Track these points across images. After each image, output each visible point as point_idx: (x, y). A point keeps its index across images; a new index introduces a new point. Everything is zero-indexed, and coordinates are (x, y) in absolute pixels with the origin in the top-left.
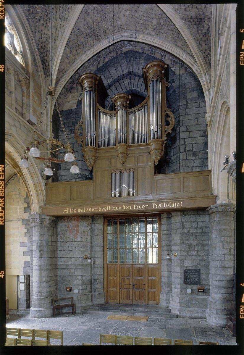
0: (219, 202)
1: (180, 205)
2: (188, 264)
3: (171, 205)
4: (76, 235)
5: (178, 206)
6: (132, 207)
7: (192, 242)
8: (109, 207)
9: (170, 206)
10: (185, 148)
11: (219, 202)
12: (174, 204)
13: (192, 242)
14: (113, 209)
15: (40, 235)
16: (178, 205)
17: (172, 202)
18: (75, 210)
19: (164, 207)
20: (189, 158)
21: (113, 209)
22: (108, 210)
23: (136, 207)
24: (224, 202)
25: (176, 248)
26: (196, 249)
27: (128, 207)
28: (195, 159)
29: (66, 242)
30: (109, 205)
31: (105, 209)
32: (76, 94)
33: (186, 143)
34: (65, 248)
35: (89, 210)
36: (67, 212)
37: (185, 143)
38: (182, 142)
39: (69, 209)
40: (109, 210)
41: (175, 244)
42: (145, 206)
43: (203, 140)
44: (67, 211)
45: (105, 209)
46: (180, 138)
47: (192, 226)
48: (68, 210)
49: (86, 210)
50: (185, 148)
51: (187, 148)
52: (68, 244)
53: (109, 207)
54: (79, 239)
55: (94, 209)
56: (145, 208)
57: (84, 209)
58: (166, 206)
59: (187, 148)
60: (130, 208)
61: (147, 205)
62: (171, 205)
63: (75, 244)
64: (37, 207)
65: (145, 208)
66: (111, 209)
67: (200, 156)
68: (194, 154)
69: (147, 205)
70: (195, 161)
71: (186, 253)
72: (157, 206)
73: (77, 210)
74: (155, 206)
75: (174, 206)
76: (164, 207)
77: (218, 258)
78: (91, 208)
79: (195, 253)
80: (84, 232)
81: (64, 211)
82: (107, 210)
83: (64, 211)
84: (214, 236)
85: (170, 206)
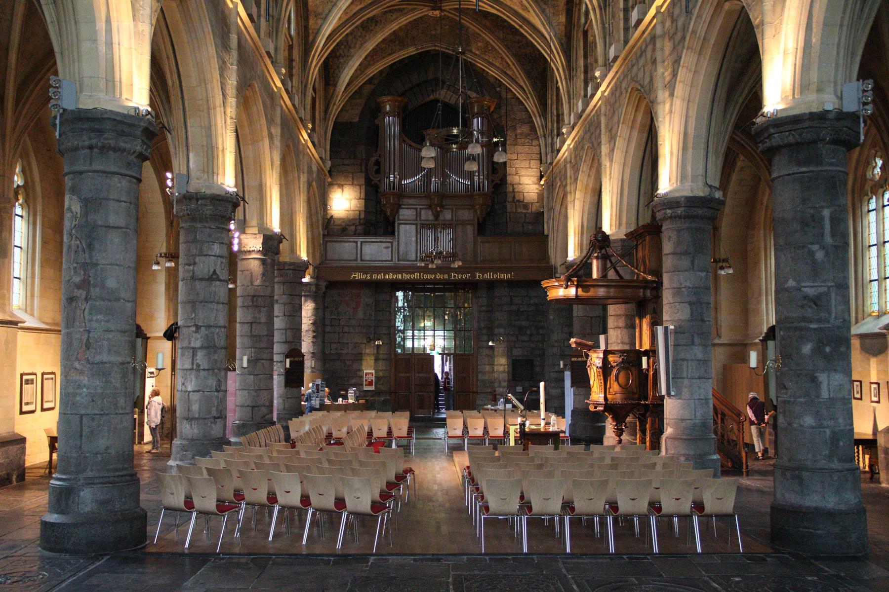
2: (516, 352)
4: (356, 309)
6: (450, 276)
7: (523, 323)
25: (502, 331)
26: (528, 332)
34: (337, 329)
41: (499, 326)
54: (360, 314)
60: (446, 276)
63: (353, 322)
71: (514, 339)
73: (371, 276)
77: (556, 344)
79: (526, 339)
80: (368, 305)
84: (551, 317)
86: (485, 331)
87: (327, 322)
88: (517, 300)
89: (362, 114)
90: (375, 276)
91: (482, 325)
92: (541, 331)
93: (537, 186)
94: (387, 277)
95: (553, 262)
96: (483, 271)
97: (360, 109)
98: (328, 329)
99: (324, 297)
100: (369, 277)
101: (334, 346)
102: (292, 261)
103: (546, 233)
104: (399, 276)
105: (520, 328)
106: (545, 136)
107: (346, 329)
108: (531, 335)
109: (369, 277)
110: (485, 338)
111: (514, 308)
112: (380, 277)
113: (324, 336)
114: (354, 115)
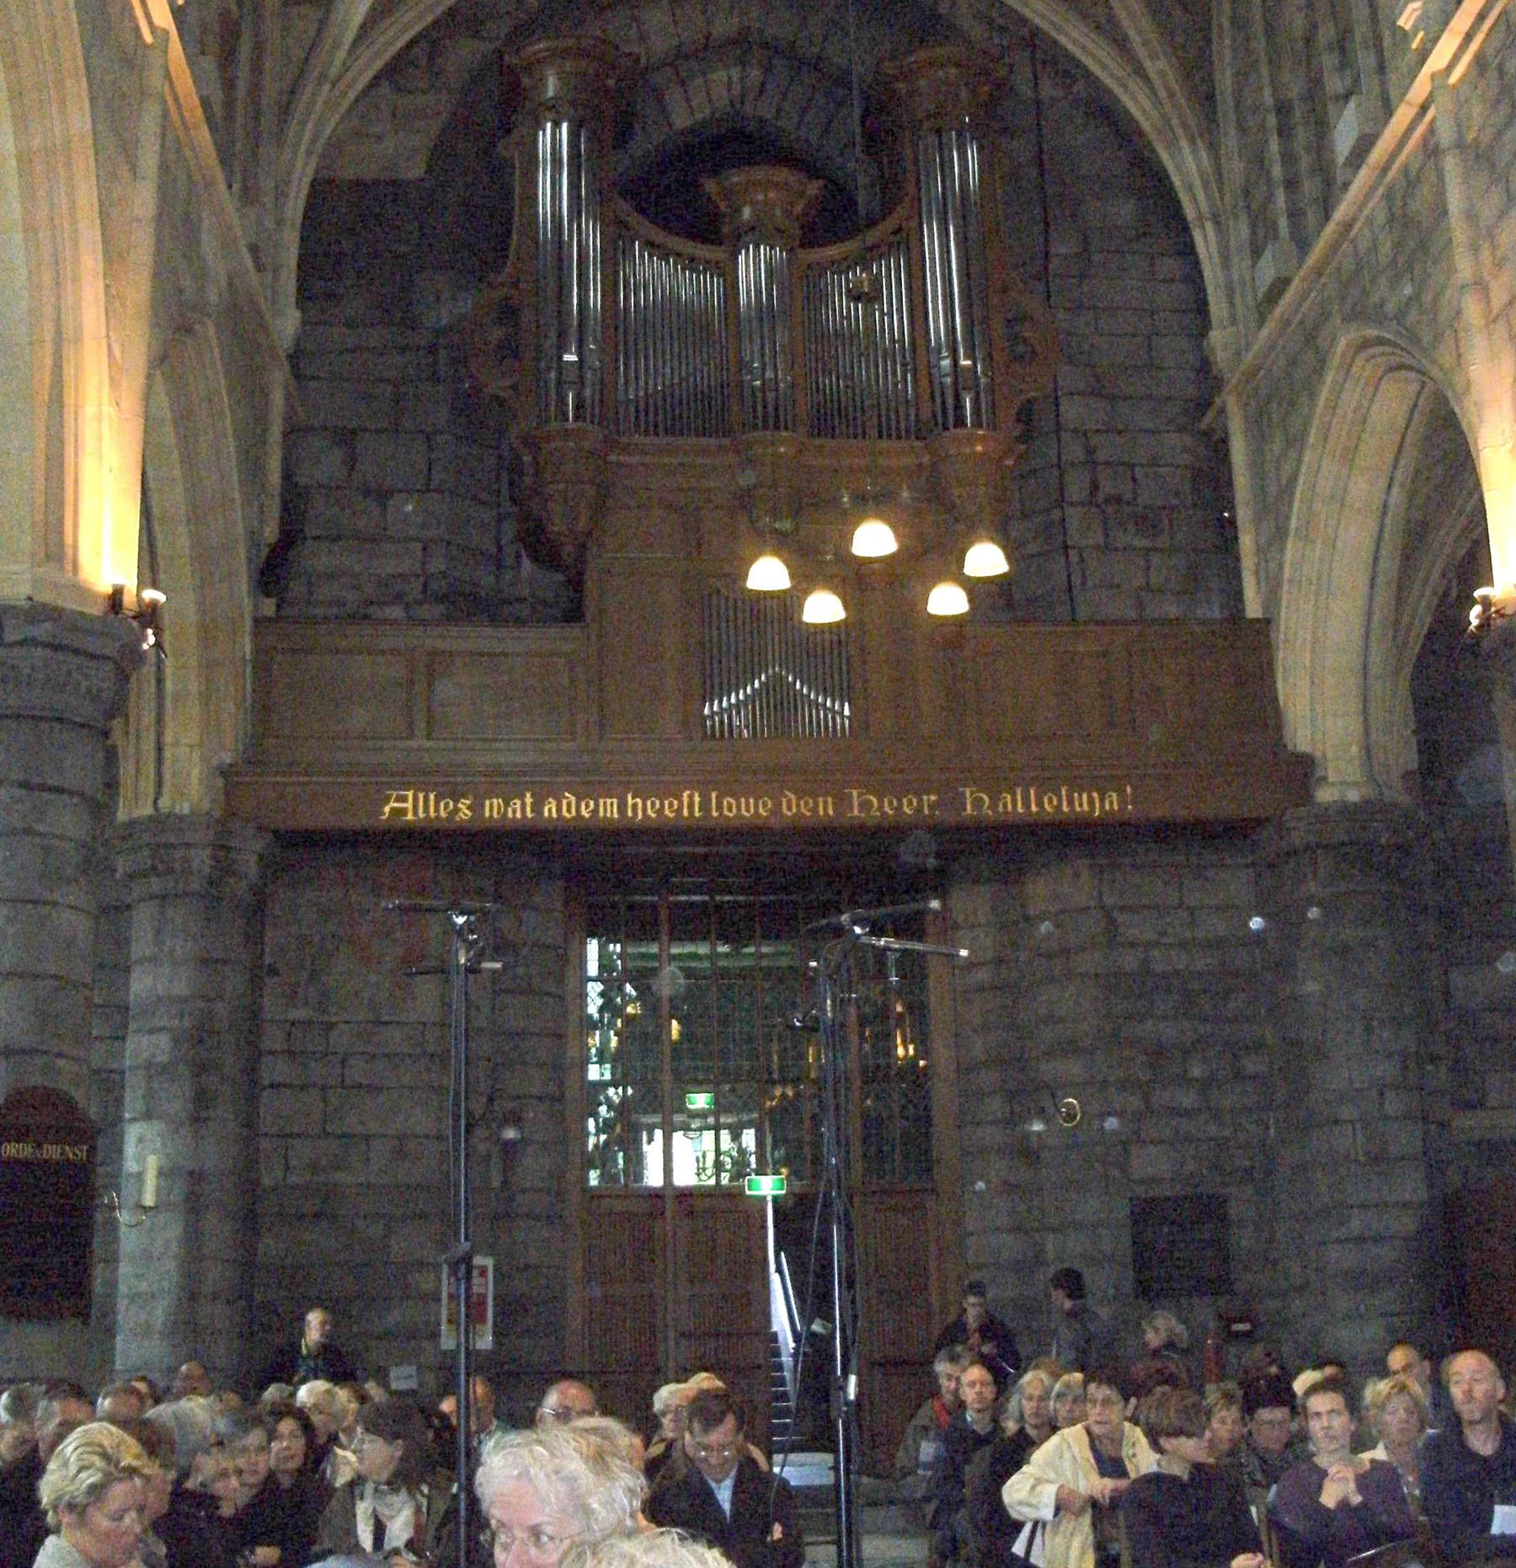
0: (1325, 795)
1: (1123, 802)
3: (1071, 803)
5: (1107, 807)
6: (842, 800)
8: (697, 799)
9: (1065, 808)
10: (1095, 487)
11: (1325, 795)
12: (1085, 796)
13: (1169, 1031)
14: (719, 807)
15: (205, 961)
16: (1111, 803)
17: (1076, 784)
18: (464, 805)
19: (1034, 808)
20: (1122, 539)
21: (719, 807)
22: (686, 813)
23: (865, 806)
24: (1353, 796)
27: (816, 804)
28: (1155, 549)
29: (331, 1026)
30: (691, 786)
31: (671, 805)
32: (421, 99)
33: (1101, 456)
35: (559, 809)
36: (410, 817)
37: (1090, 451)
38: (1074, 451)
39: (421, 796)
40: (697, 814)
42: (920, 801)
43: (1185, 450)
44: (409, 805)
45: (671, 805)
46: (1059, 428)
47: (1164, 934)
48: (416, 799)
49: (537, 807)
50: (1095, 487)
51: (1107, 487)
52: (340, 1040)
53: (697, 799)
55: (597, 805)
56: (919, 810)
57: (529, 800)
58: (1040, 804)
59: (1107, 487)
60: (826, 808)
61: (933, 798)
62: (1071, 803)
63: (393, 1038)
64: (195, 773)
65: (919, 810)
66: (705, 806)
67: (1179, 536)
68: (1146, 523)
69: (933, 798)
70: (1156, 559)
72: (993, 806)
73: (476, 808)
74: (978, 803)
75: (1086, 807)
76: (1034, 808)
78: (573, 799)
81: (387, 809)
82: (679, 810)
83: (387, 809)
84: (1312, 987)
85: (1065, 808)
86: (987, 1078)
87: (273, 1039)
88: (1137, 928)
89: (440, 153)
90: (493, 808)
91: (978, 1047)
92: (1251, 1065)
93: (1188, 440)
94: (550, 809)
95: (1300, 737)
96: (995, 783)
97: (435, 127)
98: (274, 1070)
99: (257, 911)
100: (465, 813)
101: (302, 1151)
102: (45, 597)
103: (1253, 608)
104: (609, 809)
105: (1158, 1054)
106: (1215, 219)
107: (358, 1071)
108: (1206, 1085)
109: (465, 813)
110: (996, 1106)
111: (1130, 961)
112: (520, 810)
113: (252, 1099)
114: (402, 152)
